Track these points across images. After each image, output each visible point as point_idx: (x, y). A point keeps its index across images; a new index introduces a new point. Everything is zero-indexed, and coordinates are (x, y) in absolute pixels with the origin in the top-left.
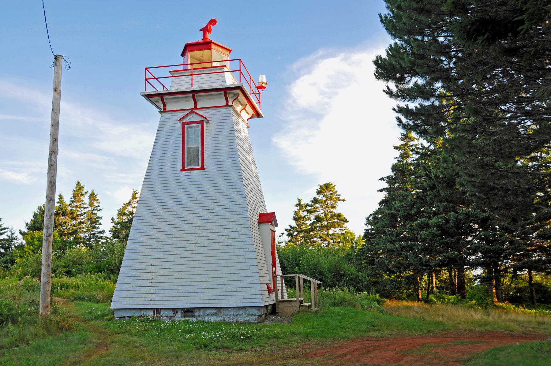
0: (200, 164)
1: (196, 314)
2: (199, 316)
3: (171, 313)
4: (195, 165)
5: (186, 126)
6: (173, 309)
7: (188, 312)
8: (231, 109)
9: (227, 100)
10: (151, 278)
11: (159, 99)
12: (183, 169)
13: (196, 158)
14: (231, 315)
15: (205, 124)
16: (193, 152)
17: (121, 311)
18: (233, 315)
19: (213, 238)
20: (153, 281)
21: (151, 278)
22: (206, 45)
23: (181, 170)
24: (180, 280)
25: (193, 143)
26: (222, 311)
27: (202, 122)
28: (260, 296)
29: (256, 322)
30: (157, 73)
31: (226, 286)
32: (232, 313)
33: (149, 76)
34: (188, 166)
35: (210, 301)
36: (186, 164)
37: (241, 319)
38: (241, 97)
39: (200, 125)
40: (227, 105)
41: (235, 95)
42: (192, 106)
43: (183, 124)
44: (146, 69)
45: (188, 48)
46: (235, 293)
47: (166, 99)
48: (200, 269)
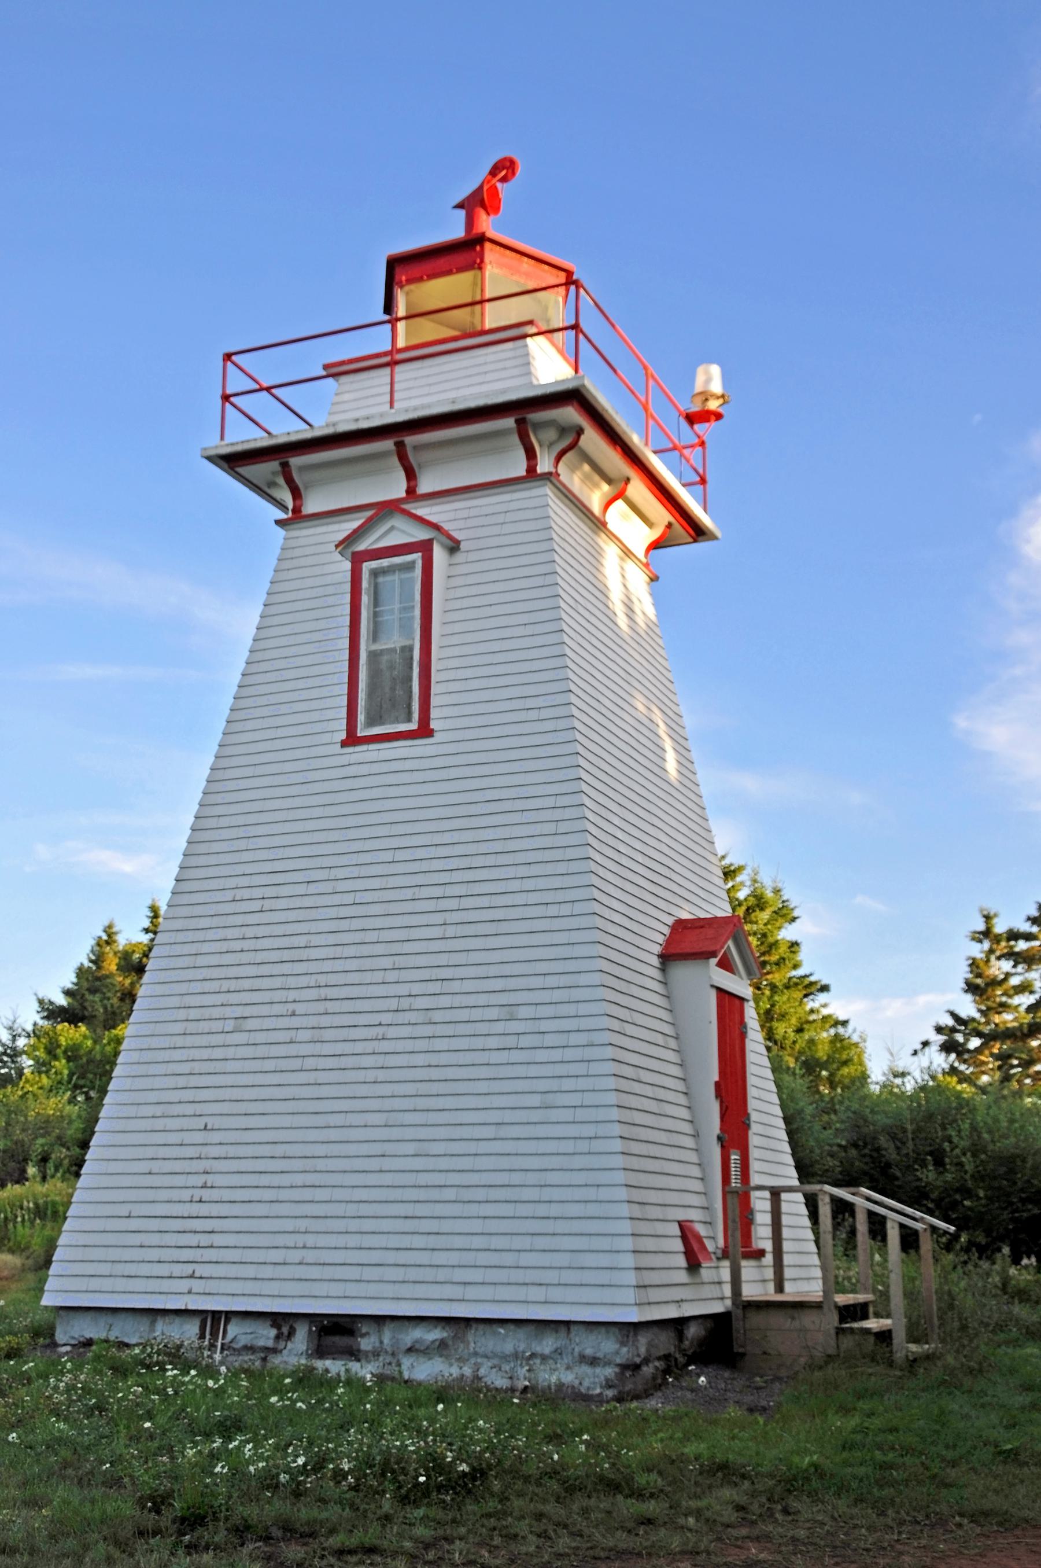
0: (416, 716)
1: (366, 1344)
2: (376, 1354)
3: (266, 1335)
4: (397, 721)
5: (367, 566)
6: (276, 1319)
7: (335, 1332)
8: (548, 490)
9: (531, 454)
10: (199, 1180)
11: (270, 465)
12: (352, 739)
13: (399, 692)
14: (505, 1358)
15: (438, 553)
16: (392, 668)
17: (79, 1315)
18: (516, 1356)
19: (449, 1016)
20: (206, 1194)
21: (199, 1180)
22: (466, 252)
23: (344, 744)
24: (307, 1194)
25: (399, 636)
26: (470, 1335)
27: (425, 548)
28: (631, 1278)
29: (610, 1393)
30: (267, 368)
31: (493, 1226)
32: (508, 1347)
33: (237, 382)
34: (371, 722)
35: (421, 1291)
36: (361, 718)
37: (549, 1376)
38: (592, 440)
39: (417, 557)
40: (531, 470)
41: (563, 431)
42: (397, 489)
43: (358, 559)
44: (228, 357)
45: (401, 268)
46: (526, 1259)
47: (302, 469)
48: (388, 1148)
